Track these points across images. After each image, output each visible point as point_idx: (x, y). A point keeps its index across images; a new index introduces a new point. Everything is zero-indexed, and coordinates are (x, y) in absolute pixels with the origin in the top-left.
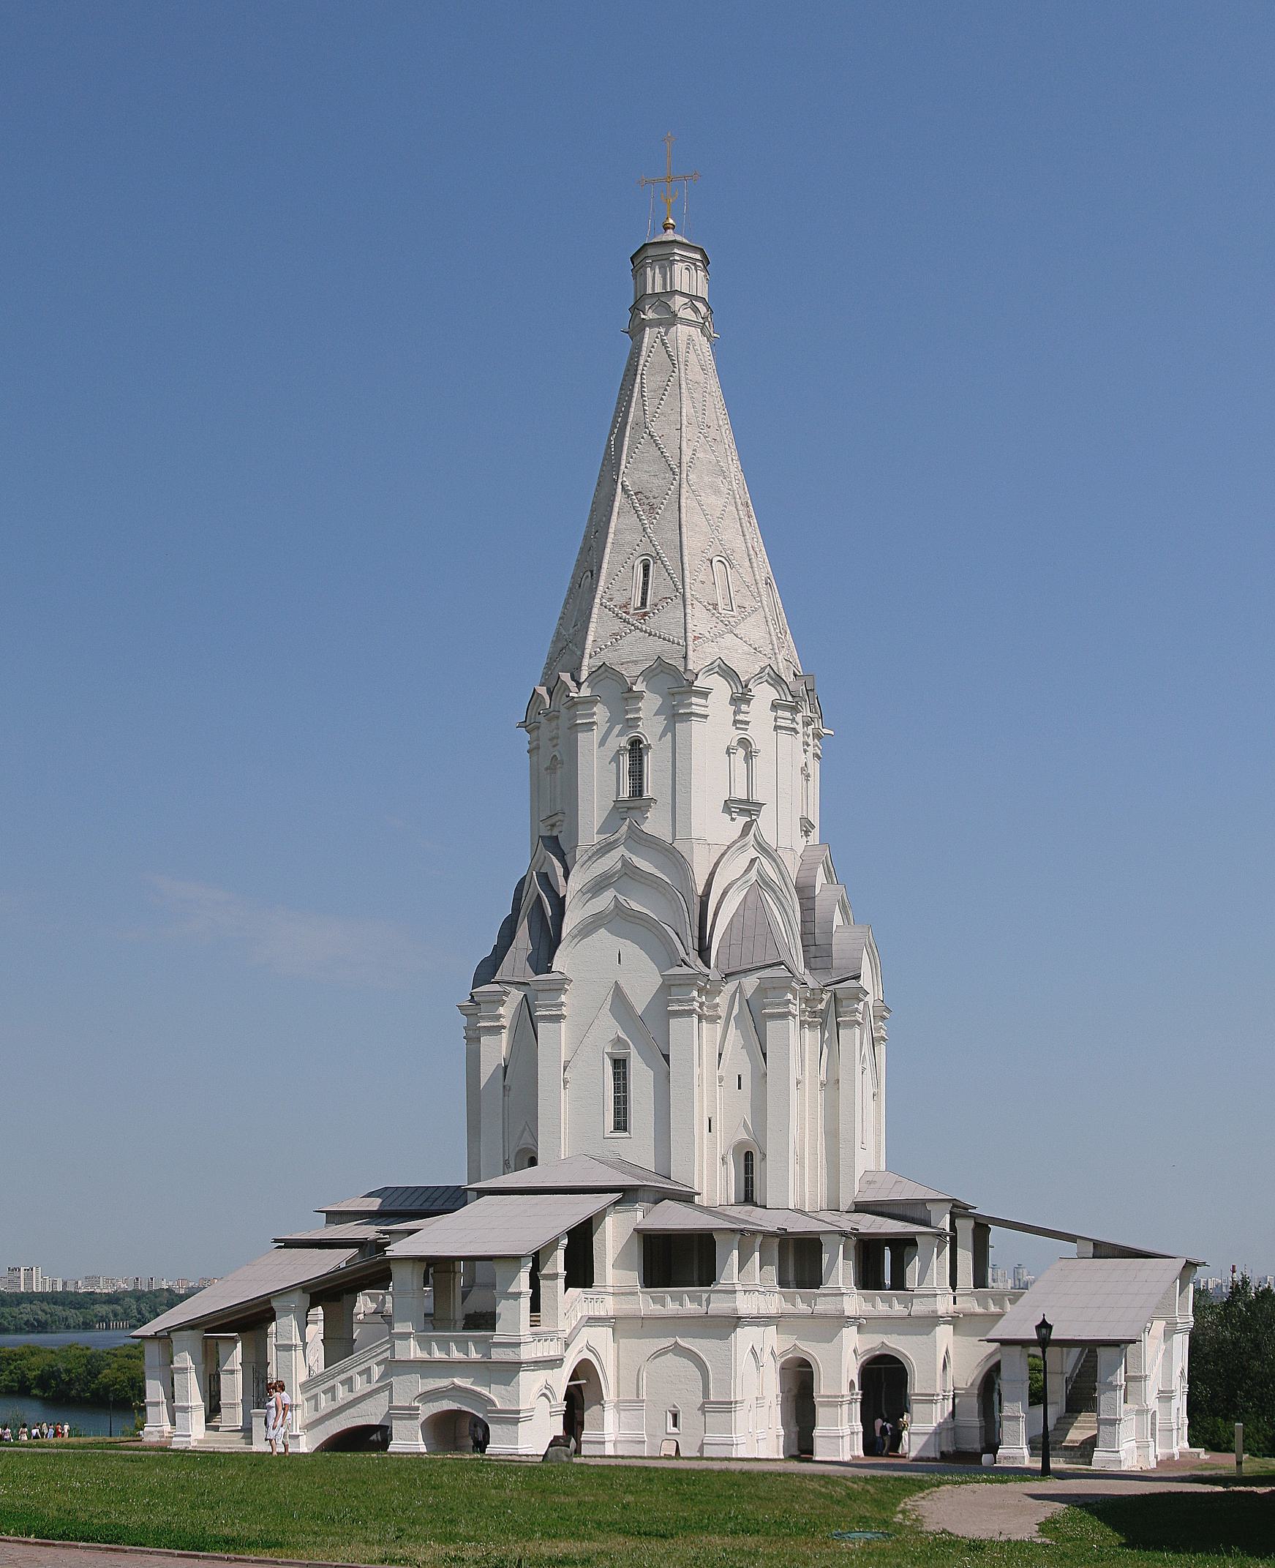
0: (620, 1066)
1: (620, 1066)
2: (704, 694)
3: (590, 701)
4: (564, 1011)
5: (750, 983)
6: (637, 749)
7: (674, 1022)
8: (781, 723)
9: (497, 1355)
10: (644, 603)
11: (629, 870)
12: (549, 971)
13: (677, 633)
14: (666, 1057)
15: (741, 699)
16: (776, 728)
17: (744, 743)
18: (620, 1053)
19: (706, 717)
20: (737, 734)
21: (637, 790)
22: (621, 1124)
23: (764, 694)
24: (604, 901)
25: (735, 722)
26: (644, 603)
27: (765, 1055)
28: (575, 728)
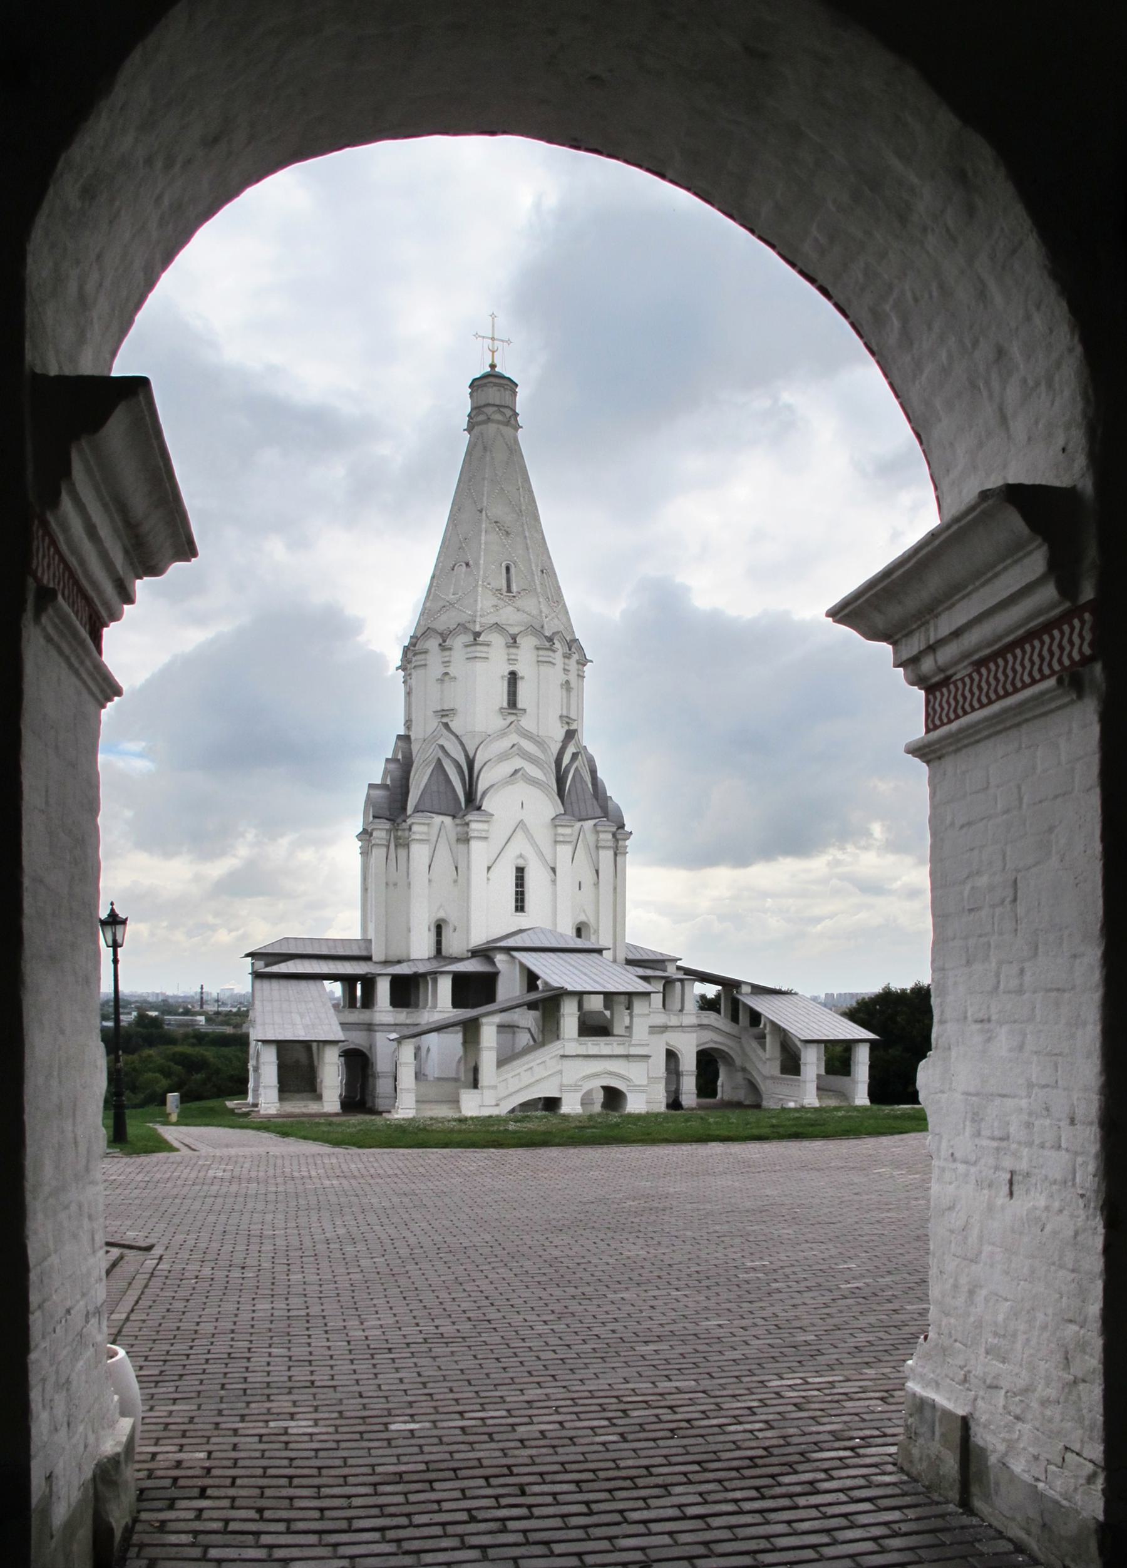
0: (520, 872)
1: (520, 872)
6: (513, 678)
7: (559, 847)
9: (633, 1051)
12: (479, 808)
13: (535, 612)
14: (554, 870)
17: (567, 682)
18: (521, 863)
21: (512, 702)
22: (520, 907)
23: (576, 657)
24: (507, 768)
25: (564, 669)
26: (509, 590)
27: (597, 872)
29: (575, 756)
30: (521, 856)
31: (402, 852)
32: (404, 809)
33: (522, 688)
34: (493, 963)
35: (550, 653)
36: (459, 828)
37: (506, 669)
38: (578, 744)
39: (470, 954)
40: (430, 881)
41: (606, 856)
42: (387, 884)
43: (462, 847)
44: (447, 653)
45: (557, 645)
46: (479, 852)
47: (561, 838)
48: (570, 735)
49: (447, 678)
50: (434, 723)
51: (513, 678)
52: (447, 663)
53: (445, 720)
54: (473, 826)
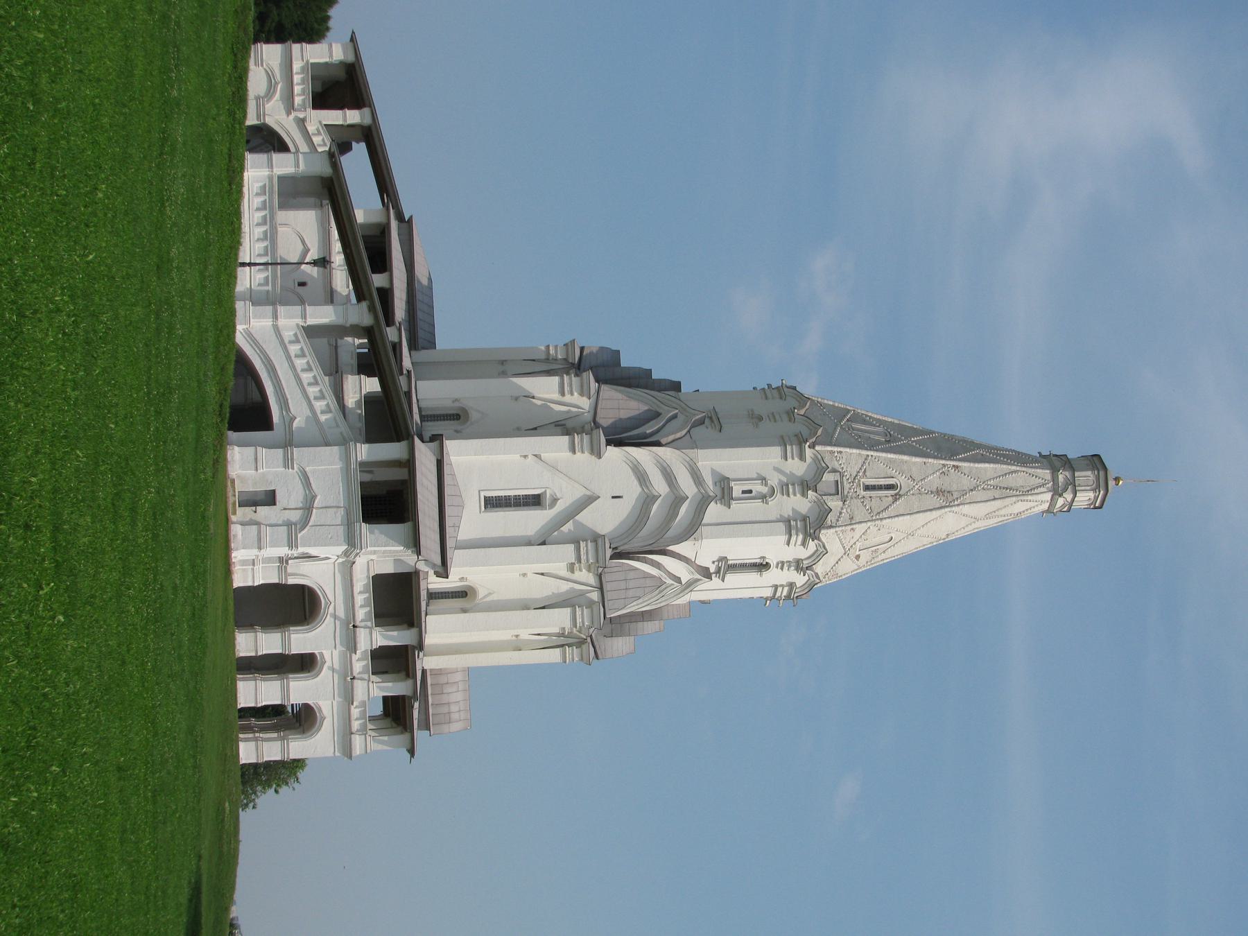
0: (535, 501)
1: (535, 501)
2: (804, 544)
3: (802, 457)
4: (578, 454)
5: (595, 596)
7: (571, 547)
8: (780, 589)
10: (867, 488)
11: (678, 500)
15: (799, 566)
16: (776, 587)
19: (788, 544)
20: (773, 563)
22: (493, 503)
23: (800, 580)
25: (783, 563)
27: (543, 608)
28: (783, 442)
29: (678, 580)
30: (555, 501)
35: (801, 537)
38: (691, 584)
40: (517, 399)
41: (559, 620)
42: (503, 362)
44: (785, 417)
45: (812, 545)
46: (555, 447)
48: (706, 573)
52: (773, 417)
53: (707, 421)
54: (586, 438)
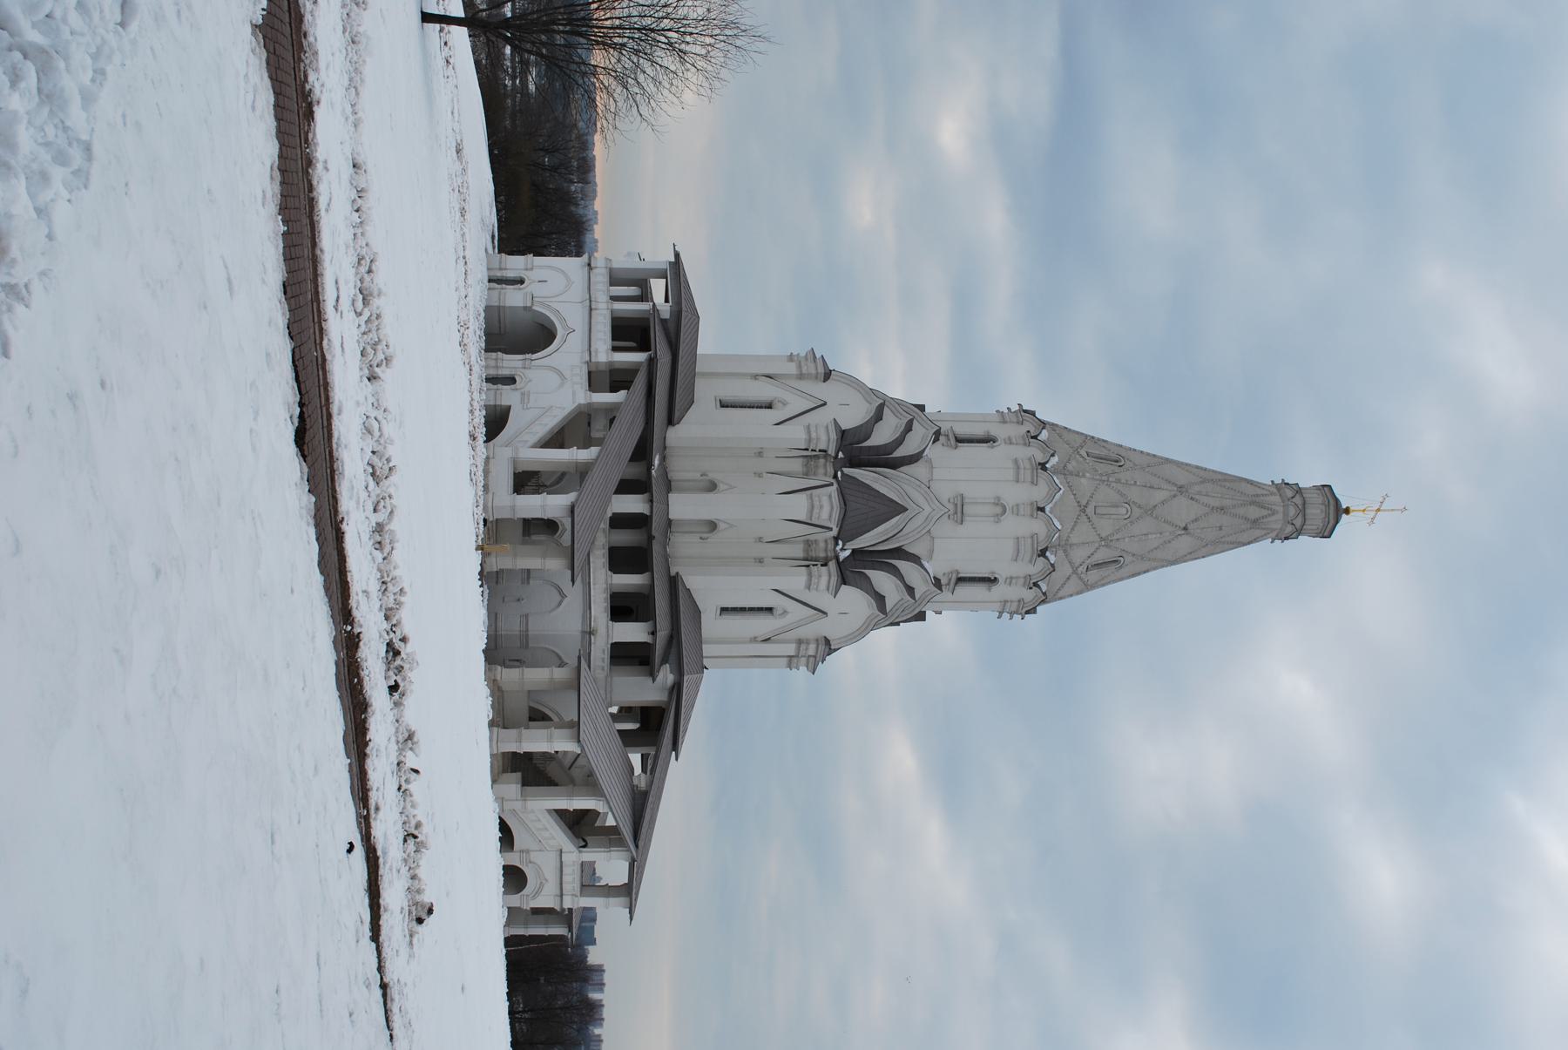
0: (770, 610)
6: (990, 581)
18: (777, 612)
30: (785, 612)
31: (797, 466)
32: (852, 466)
33: (977, 591)
34: (664, 661)
36: (822, 545)
37: (1001, 577)
39: (673, 573)
43: (798, 551)
44: (1028, 511)
47: (803, 647)
49: (999, 510)
50: (945, 491)
51: (990, 581)
52: (1016, 510)
